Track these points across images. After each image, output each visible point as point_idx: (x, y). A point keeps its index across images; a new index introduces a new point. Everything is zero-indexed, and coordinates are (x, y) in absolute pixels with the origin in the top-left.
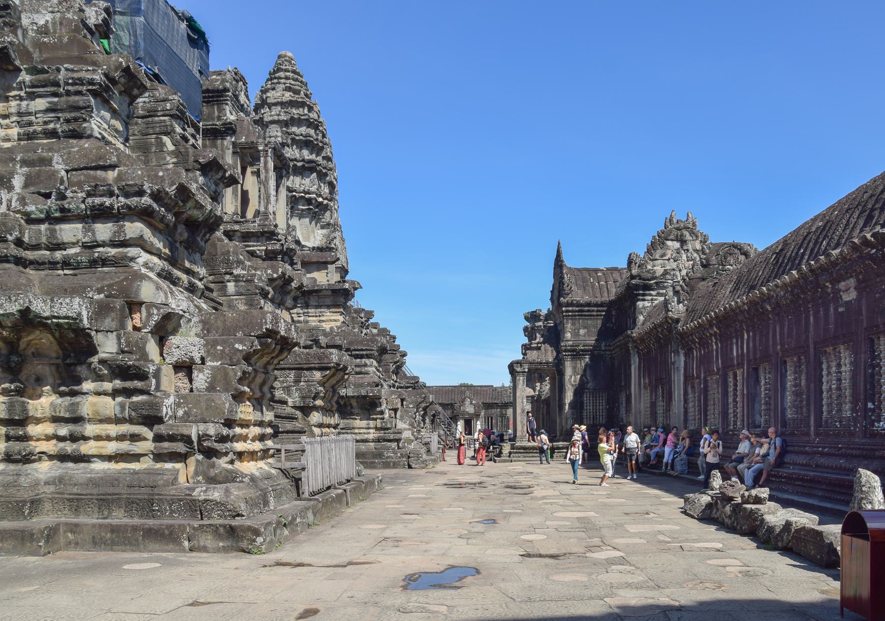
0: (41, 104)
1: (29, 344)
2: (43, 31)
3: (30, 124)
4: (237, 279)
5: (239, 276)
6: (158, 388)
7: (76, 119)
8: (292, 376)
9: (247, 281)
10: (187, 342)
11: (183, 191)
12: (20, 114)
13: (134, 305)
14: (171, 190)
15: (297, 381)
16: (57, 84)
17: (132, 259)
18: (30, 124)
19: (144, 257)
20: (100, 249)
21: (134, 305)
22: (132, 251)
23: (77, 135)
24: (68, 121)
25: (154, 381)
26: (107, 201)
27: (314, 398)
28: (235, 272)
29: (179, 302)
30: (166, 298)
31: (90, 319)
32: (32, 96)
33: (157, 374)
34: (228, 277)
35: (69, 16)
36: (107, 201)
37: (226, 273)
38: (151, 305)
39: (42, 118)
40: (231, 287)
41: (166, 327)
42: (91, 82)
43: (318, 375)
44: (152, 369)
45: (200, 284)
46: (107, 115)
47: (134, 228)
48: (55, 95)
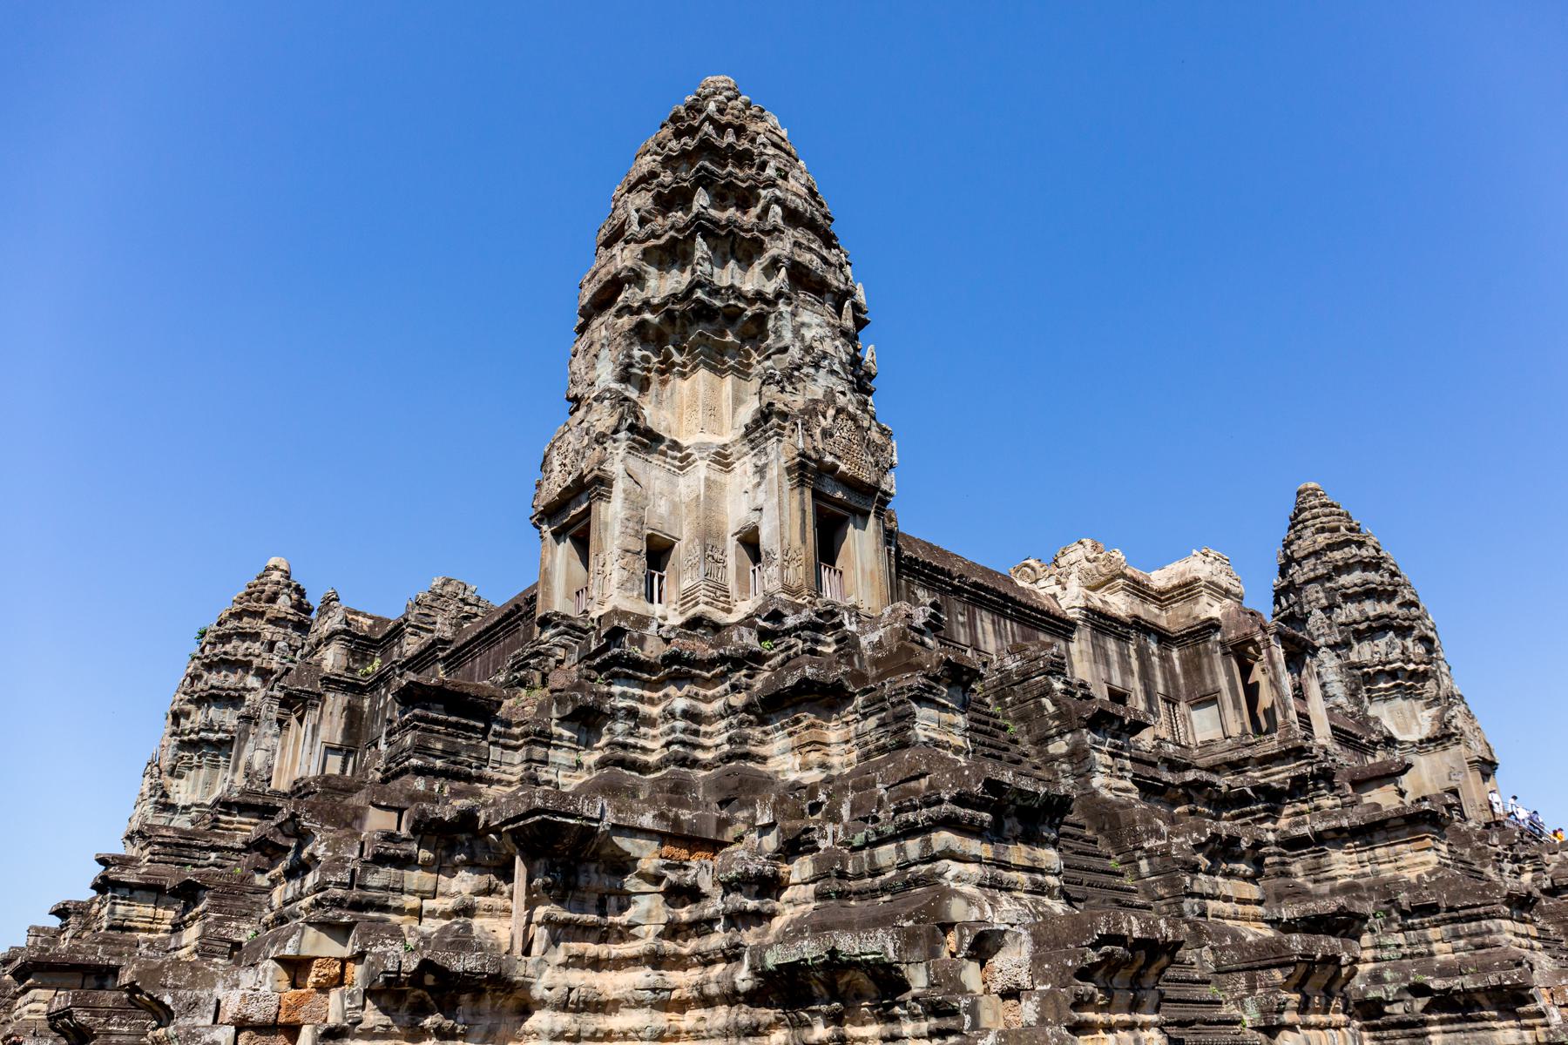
0: (872, 722)
1: (848, 984)
2: (878, 646)
3: (866, 744)
4: (1150, 854)
5: (1151, 849)
6: (975, 1025)
7: (901, 729)
8: (1243, 980)
9: (1163, 854)
10: (1013, 961)
11: (993, 785)
12: (858, 736)
13: (947, 927)
14: (977, 789)
15: (1251, 988)
16: (883, 700)
17: (941, 875)
18: (866, 744)
19: (955, 868)
20: (913, 869)
21: (947, 927)
22: (941, 865)
23: (904, 745)
24: (895, 733)
25: (968, 1018)
26: (911, 816)
27: (1280, 1012)
28: (1146, 845)
29: (1005, 912)
30: (982, 910)
31: (897, 950)
32: (865, 716)
33: (973, 1010)
34: (1138, 853)
35: (897, 625)
36: (911, 816)
37: (1135, 849)
38: (966, 924)
39: (874, 735)
40: (1144, 865)
41: (984, 946)
42: (910, 689)
43: (1278, 975)
44: (964, 1002)
45: (1052, 880)
46: (934, 713)
47: (943, 839)
48: (883, 710)
